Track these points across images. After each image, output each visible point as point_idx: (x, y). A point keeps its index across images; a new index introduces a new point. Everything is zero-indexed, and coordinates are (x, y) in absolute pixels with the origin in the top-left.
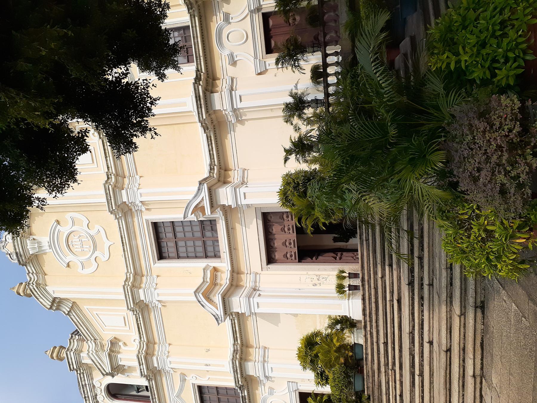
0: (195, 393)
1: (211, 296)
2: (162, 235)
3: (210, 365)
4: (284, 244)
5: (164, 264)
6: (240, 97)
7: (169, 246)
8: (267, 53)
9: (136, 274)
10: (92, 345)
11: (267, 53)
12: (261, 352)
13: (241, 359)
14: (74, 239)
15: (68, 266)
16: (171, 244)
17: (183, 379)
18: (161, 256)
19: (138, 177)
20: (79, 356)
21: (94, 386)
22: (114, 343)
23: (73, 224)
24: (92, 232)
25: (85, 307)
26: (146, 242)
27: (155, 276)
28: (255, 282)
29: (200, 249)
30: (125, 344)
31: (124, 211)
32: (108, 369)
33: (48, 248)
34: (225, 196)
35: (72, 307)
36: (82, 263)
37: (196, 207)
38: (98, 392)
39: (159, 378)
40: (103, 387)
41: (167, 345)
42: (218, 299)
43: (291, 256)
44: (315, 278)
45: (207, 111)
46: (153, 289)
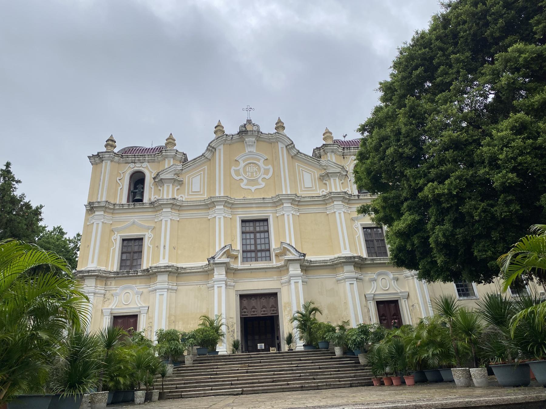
0: (137, 235)
1: (225, 255)
2: (257, 224)
3: (164, 249)
4: (254, 307)
5: (238, 224)
6: (353, 284)
7: (250, 228)
8: (377, 302)
9: (233, 204)
10: (180, 167)
11: (377, 302)
12: (175, 287)
13: (170, 272)
14: (255, 169)
15: (236, 160)
16: (252, 229)
17: (148, 228)
18: (244, 221)
19: (298, 214)
20: (171, 158)
21: (143, 162)
22: (181, 183)
23: (265, 169)
24: (260, 180)
25: (206, 167)
26: (255, 213)
27: (231, 217)
28: (230, 286)
29: (248, 248)
30: (178, 189)
31: (277, 202)
32: (162, 176)
33: (249, 150)
34: (295, 270)
35: (207, 158)
36: (239, 170)
37: (288, 250)
38: (137, 165)
39: (150, 210)
40: (140, 168)
41: (178, 219)
42: (224, 260)
43: (245, 312)
44: (232, 329)
45: (343, 262)
46: (224, 215)
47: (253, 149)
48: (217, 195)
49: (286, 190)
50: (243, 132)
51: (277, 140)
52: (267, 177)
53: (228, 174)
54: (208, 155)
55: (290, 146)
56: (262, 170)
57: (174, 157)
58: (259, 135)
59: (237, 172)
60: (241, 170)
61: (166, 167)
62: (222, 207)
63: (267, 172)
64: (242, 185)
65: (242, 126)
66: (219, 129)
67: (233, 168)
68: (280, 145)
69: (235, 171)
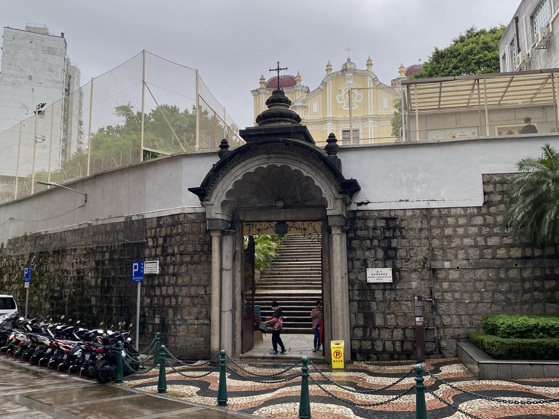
22: (306, 107)
36: (341, 97)
47: (351, 82)
48: (328, 116)
49: (371, 113)
50: (345, 70)
51: (367, 75)
52: (359, 101)
53: (334, 100)
54: (322, 87)
55: (375, 80)
56: (356, 96)
57: (301, 90)
58: (355, 72)
59: (341, 99)
60: (343, 98)
61: (297, 98)
62: (331, 123)
63: (359, 98)
64: (343, 108)
65: (343, 65)
66: (329, 68)
67: (338, 95)
68: (369, 79)
69: (339, 97)
